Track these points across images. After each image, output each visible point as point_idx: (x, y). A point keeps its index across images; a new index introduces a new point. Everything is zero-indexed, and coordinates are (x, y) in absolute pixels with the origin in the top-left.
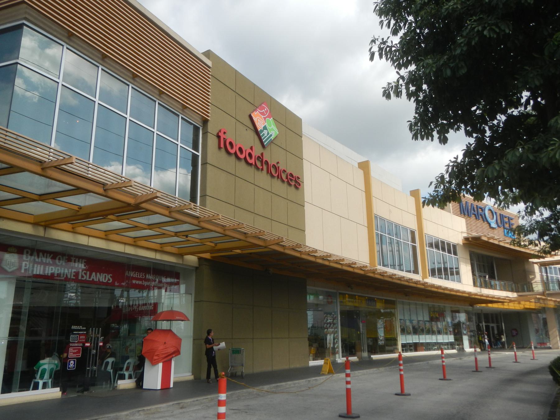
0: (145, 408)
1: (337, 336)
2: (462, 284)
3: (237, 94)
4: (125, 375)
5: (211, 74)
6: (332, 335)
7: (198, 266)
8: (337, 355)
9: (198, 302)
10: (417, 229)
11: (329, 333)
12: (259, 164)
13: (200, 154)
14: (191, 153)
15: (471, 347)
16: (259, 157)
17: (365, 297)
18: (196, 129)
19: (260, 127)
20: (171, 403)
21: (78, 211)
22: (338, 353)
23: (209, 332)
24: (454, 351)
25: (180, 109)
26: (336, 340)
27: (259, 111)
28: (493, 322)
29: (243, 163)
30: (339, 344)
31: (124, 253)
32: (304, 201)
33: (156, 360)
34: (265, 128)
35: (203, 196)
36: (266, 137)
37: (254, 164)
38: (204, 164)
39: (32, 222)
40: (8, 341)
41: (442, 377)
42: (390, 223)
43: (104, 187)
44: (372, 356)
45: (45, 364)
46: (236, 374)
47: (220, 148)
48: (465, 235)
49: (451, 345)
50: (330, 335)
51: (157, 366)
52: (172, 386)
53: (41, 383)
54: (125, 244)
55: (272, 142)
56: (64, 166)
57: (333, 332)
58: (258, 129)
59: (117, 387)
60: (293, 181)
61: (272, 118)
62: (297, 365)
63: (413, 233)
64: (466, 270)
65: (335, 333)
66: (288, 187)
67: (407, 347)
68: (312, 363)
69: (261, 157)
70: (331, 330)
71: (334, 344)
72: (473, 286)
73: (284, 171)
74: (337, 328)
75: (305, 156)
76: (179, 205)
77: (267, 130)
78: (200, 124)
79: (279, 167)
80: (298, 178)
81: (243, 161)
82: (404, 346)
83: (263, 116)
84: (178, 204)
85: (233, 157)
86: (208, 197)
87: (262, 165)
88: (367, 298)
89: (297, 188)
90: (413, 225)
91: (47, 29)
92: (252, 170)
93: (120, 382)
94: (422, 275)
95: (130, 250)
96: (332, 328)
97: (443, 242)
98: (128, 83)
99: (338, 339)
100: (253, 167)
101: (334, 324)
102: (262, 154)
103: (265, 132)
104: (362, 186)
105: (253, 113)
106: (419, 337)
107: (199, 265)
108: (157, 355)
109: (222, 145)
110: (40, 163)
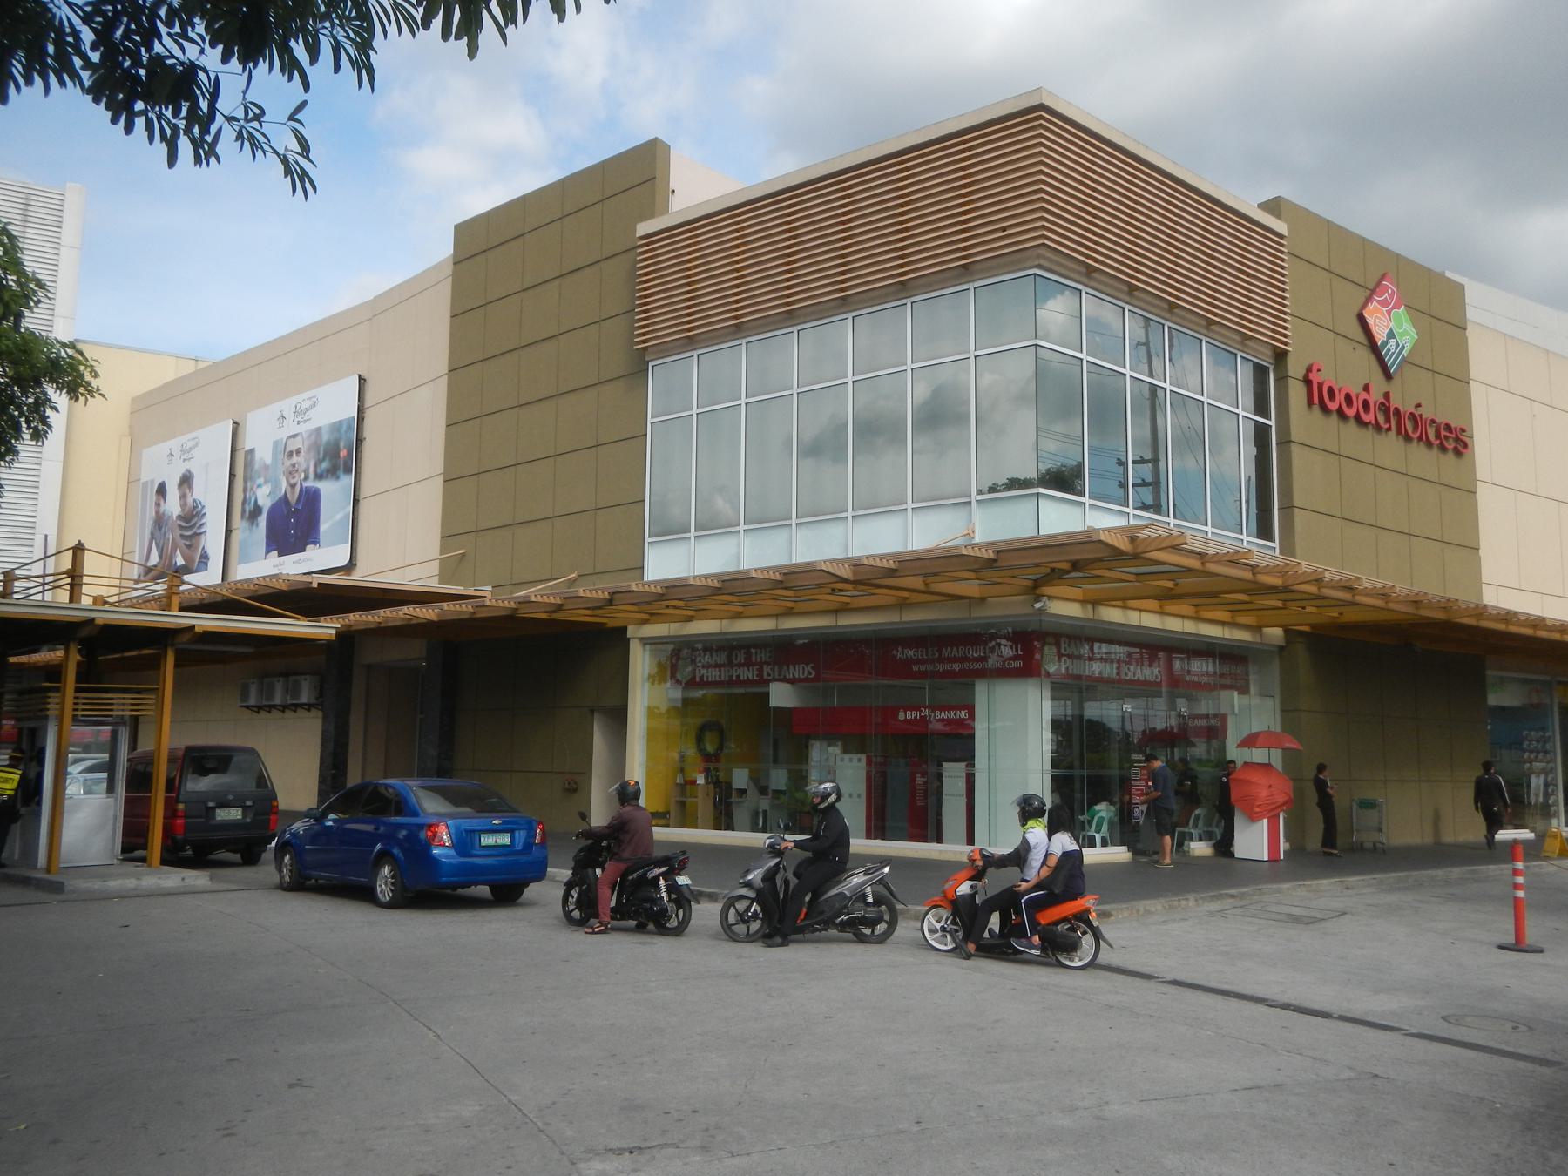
0: (1306, 883)
1: (1553, 779)
4: (1215, 833)
6: (1542, 778)
7: (1284, 644)
11: (1534, 772)
12: (1381, 419)
13: (1272, 423)
14: (1253, 423)
16: (1382, 404)
18: (1260, 373)
19: (1380, 335)
20: (1333, 880)
21: (1172, 589)
22: (1556, 815)
25: (1237, 342)
26: (1551, 787)
27: (1378, 301)
29: (1352, 424)
30: (1558, 797)
31: (1183, 633)
32: (1475, 480)
33: (1257, 813)
34: (1391, 335)
35: (1287, 508)
36: (1393, 353)
37: (1373, 422)
38: (1285, 442)
40: (1054, 778)
43: (1252, 571)
46: (1362, 845)
47: (1310, 402)
50: (1538, 776)
51: (1257, 826)
52: (1282, 857)
54: (1183, 617)
58: (1377, 339)
59: (1189, 852)
60: (1451, 441)
61: (1403, 307)
65: (1545, 771)
66: (1441, 455)
69: (1385, 402)
70: (1538, 765)
71: (1547, 795)
73: (1433, 421)
74: (1554, 760)
75: (1474, 371)
77: (1395, 337)
78: (1267, 360)
79: (1421, 416)
80: (1463, 430)
83: (1384, 309)
85: (1335, 416)
86: (1296, 510)
87: (1388, 420)
89: (1458, 453)
92: (1369, 433)
93: (1193, 845)
95: (1189, 627)
99: (1556, 785)
100: (1370, 427)
101: (1546, 752)
102: (1387, 395)
103: (1392, 343)
105: (1367, 309)
108: (1259, 806)
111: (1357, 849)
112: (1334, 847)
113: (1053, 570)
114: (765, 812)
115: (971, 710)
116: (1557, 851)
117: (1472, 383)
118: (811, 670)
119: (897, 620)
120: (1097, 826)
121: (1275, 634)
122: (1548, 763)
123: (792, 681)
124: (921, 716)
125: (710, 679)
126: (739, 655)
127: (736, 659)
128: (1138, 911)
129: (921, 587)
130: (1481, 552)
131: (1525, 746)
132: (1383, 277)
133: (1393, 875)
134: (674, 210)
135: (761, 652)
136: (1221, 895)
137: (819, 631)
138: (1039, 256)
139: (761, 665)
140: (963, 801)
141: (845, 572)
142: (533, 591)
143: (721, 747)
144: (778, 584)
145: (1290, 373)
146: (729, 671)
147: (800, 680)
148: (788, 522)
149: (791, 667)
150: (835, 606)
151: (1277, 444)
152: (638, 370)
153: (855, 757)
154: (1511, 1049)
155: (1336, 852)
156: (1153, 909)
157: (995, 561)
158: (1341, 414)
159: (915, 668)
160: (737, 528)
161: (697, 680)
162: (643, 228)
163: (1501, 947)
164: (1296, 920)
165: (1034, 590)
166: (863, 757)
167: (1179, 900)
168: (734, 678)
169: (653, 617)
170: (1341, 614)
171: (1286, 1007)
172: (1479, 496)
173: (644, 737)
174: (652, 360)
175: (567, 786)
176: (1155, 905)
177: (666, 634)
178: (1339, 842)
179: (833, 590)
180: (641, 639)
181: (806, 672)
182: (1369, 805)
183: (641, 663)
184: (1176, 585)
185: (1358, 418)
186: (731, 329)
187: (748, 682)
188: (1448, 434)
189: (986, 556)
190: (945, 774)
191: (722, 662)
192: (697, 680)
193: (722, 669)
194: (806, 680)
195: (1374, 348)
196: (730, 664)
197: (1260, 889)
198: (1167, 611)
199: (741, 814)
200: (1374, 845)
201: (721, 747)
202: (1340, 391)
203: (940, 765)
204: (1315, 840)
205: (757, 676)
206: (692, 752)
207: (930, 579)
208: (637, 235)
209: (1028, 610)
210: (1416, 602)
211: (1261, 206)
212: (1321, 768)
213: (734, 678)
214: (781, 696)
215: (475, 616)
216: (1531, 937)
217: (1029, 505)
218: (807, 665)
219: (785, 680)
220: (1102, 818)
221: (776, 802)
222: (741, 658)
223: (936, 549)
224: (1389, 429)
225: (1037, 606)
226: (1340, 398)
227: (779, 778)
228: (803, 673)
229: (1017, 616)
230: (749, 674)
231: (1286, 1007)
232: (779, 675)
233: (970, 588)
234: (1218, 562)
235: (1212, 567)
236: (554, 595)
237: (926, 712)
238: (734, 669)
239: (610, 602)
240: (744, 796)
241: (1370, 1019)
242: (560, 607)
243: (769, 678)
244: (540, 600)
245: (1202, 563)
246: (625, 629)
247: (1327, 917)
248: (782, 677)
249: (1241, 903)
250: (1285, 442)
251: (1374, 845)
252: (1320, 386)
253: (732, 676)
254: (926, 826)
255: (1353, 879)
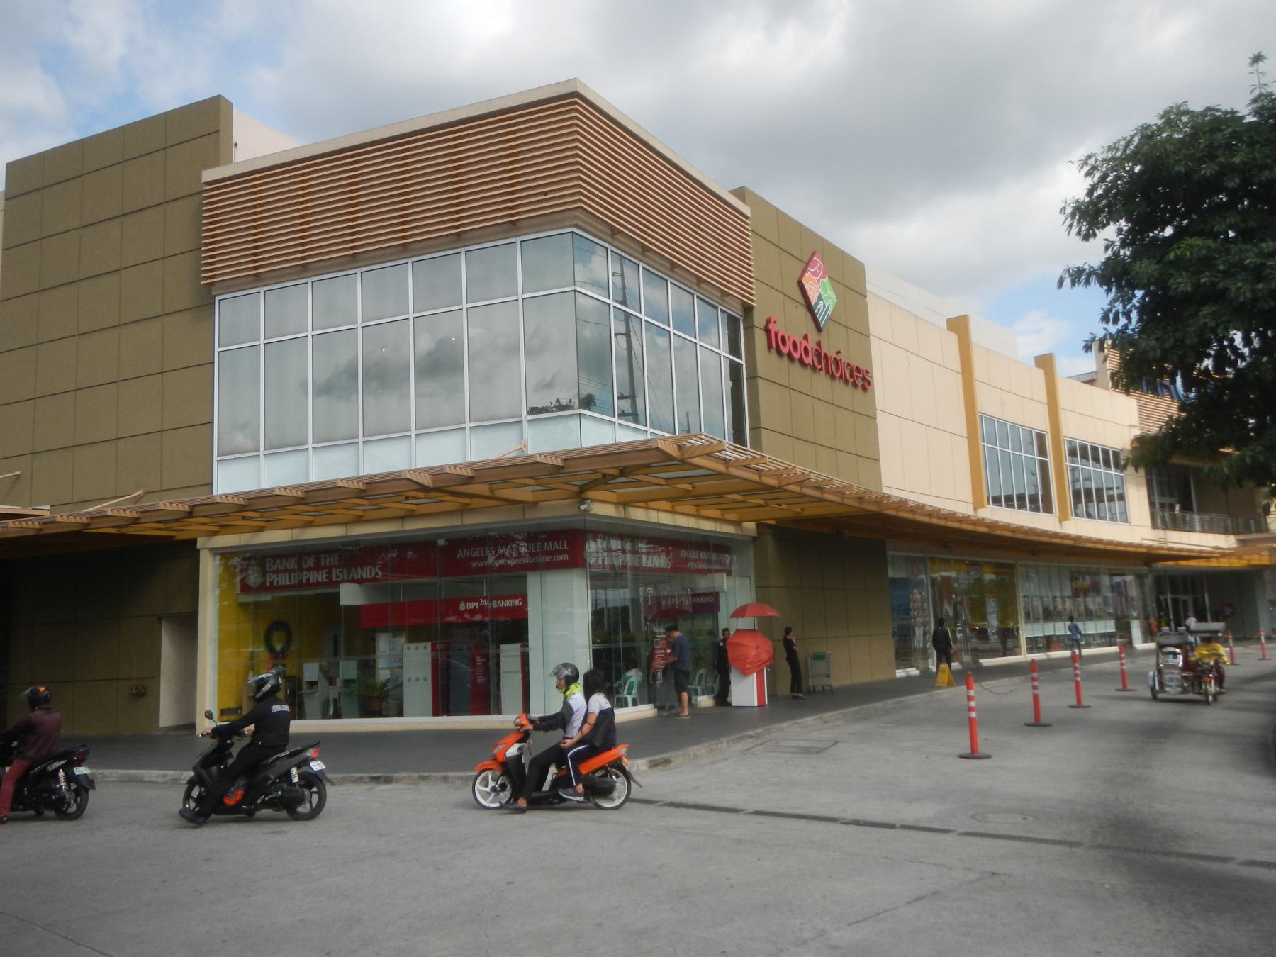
2: (1130, 525)
3: (781, 251)
5: (750, 229)
6: (922, 628)
7: (756, 535)
8: (930, 661)
9: (761, 588)
10: (1048, 430)
13: (743, 362)
15: (1145, 641)
16: (816, 350)
17: (965, 561)
18: (732, 323)
19: (813, 299)
20: (815, 717)
21: (691, 491)
23: (788, 631)
24: (1115, 649)
25: (718, 297)
27: (811, 272)
28: (1186, 593)
34: (820, 298)
35: (756, 428)
36: (822, 312)
37: (811, 363)
39: (615, 501)
41: (1121, 687)
42: (1003, 424)
43: (759, 474)
44: (981, 661)
45: (631, 677)
46: (814, 688)
47: (770, 347)
48: (1137, 432)
49: (1108, 639)
51: (749, 678)
52: (766, 703)
53: (630, 699)
54: (688, 515)
55: (829, 319)
56: (717, 454)
57: (923, 622)
59: (696, 704)
61: (827, 277)
62: (879, 676)
63: (1041, 437)
64: (1137, 498)
66: (853, 389)
67: (1034, 645)
68: (900, 673)
70: (920, 620)
72: (1150, 529)
73: (849, 365)
75: (874, 329)
76: (708, 443)
77: (822, 300)
79: (841, 360)
80: (867, 372)
81: (797, 363)
82: (1029, 640)
84: (706, 440)
85: (785, 358)
87: (820, 363)
88: (967, 562)
89: (864, 389)
90: (1043, 425)
91: (590, 229)
92: (808, 372)
94: (1060, 515)
95: (692, 523)
96: (921, 617)
97: (1095, 449)
98: (666, 277)
100: (809, 367)
101: (924, 610)
103: (821, 304)
104: (957, 366)
105: (805, 277)
106: (1054, 626)
107: (759, 533)
108: (750, 663)
109: (774, 345)
110: (723, 462)
111: (812, 692)
112: (800, 691)
113: (604, 475)
114: (335, 701)
115: (524, 598)
116: (946, 681)
117: (871, 337)
118: (377, 570)
119: (459, 523)
120: (628, 689)
121: (750, 527)
122: (925, 618)
123: (360, 582)
124: (479, 606)
125: (280, 584)
126: (308, 560)
127: (306, 564)
128: (689, 756)
129: (487, 493)
130: (881, 462)
131: (911, 606)
132: (813, 254)
133: (851, 709)
134: (236, 161)
135: (330, 557)
136: (743, 736)
137: (385, 536)
138: (576, 217)
139: (329, 569)
140: (519, 676)
141: (426, 480)
142: (108, 506)
143: (288, 642)
144: (361, 494)
145: (756, 324)
146: (298, 575)
147: (368, 580)
148: (355, 440)
149: (359, 569)
150: (401, 513)
151: (747, 379)
152: (204, 303)
153: (421, 645)
154: (1037, 836)
155: (801, 695)
156: (699, 753)
157: (562, 468)
158: (790, 357)
159: (474, 565)
160: (306, 447)
161: (268, 584)
162: (208, 175)
163: (962, 757)
164: (806, 751)
165: (580, 495)
166: (429, 645)
167: (716, 744)
168: (304, 582)
169: (224, 528)
170: (802, 510)
171: (856, 823)
172: (878, 421)
173: (215, 640)
174: (219, 295)
175: (134, 692)
176: (700, 749)
177: (237, 544)
178: (804, 685)
179: (407, 498)
180: (211, 550)
181: (373, 573)
182: (820, 657)
183: (209, 570)
184: (694, 487)
185: (801, 360)
186: (299, 268)
187: (318, 584)
188: (857, 374)
189: (555, 463)
190: (502, 654)
191: (292, 567)
192: (268, 584)
193: (293, 574)
194: (374, 579)
195: (810, 308)
196: (301, 569)
197: (769, 729)
198: (679, 511)
199: (312, 704)
200: (823, 688)
201: (288, 642)
202: (789, 339)
203: (499, 648)
204: (785, 686)
205: (327, 578)
206: (261, 649)
207: (494, 487)
208: (203, 181)
209: (572, 511)
210: (860, 498)
211: (731, 192)
212: (788, 631)
213: (304, 582)
214: (350, 595)
215: (41, 533)
216: (982, 749)
217: (574, 423)
218: (375, 568)
219: (353, 581)
220: (633, 682)
221: (347, 690)
222: (311, 562)
223: (500, 460)
224: (821, 370)
225: (583, 507)
226: (789, 344)
227: (348, 669)
228: (371, 574)
229: (566, 517)
230: (321, 576)
231: (856, 823)
232: (348, 576)
233: (525, 494)
234: (736, 467)
235: (733, 471)
236: (131, 510)
237: (484, 603)
238: (305, 572)
239: (190, 514)
240: (315, 687)
241: (923, 825)
242: (136, 521)
243: (338, 579)
244: (116, 513)
245: (727, 467)
246: (194, 541)
247: (826, 746)
248: (350, 578)
249: (759, 742)
250: (753, 377)
251: (823, 688)
252: (776, 335)
253: (302, 580)
254: (485, 701)
255: (827, 715)
